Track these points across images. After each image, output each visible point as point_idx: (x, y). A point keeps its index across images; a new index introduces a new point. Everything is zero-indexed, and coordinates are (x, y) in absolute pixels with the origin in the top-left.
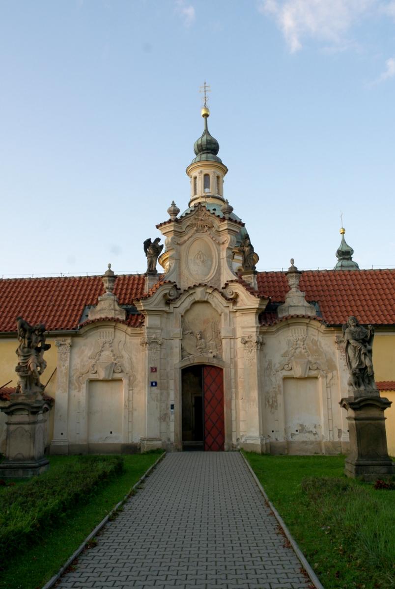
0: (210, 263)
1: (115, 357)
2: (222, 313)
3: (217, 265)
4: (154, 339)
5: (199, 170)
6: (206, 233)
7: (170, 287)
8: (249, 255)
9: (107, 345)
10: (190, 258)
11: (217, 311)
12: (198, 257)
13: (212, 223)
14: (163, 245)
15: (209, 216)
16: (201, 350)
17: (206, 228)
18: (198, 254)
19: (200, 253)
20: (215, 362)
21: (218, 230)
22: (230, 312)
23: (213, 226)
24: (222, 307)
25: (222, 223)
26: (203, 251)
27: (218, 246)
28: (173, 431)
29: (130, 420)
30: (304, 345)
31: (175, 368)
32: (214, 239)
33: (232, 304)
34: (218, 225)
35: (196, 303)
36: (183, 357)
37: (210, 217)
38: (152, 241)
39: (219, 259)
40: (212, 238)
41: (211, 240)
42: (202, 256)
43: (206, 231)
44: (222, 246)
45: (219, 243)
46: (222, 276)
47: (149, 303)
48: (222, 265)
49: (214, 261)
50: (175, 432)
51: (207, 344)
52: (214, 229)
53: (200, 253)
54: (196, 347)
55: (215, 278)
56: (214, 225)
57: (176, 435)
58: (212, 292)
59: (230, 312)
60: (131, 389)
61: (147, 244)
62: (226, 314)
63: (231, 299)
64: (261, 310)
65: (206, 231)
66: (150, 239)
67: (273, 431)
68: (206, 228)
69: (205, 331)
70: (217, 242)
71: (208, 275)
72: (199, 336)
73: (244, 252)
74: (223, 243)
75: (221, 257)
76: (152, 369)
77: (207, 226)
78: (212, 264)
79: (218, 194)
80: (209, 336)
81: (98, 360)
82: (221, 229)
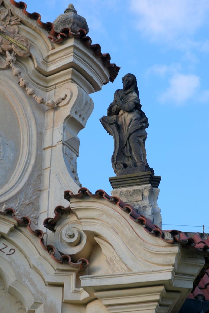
0: (10, 154)
2: (37, 304)
3: (33, 162)
6: (7, 72)
8: (137, 130)
11: (20, 302)
13: (30, 45)
15: (22, 22)
21: (43, 67)
22: (65, 303)
23: (31, 57)
24: (41, 285)
25: (58, 48)
27: (37, 113)
32: (29, 90)
33: (73, 277)
34: (45, 55)
37: (22, 26)
39: (41, 149)
40: (24, 88)
41: (20, 92)
43: (9, 67)
44: (51, 114)
45: (42, 102)
46: (44, 196)
48: (47, 164)
49: (24, 151)
52: (31, 66)
55: (22, 197)
56: (33, 52)
58: (11, 231)
59: (65, 303)
62: (50, 311)
63: (74, 258)
64: (177, 297)
65: (9, 67)
68: (10, 57)
70: (39, 99)
73: (119, 127)
74: (55, 107)
75: (47, 143)
77: (11, 51)
82: (52, 68)
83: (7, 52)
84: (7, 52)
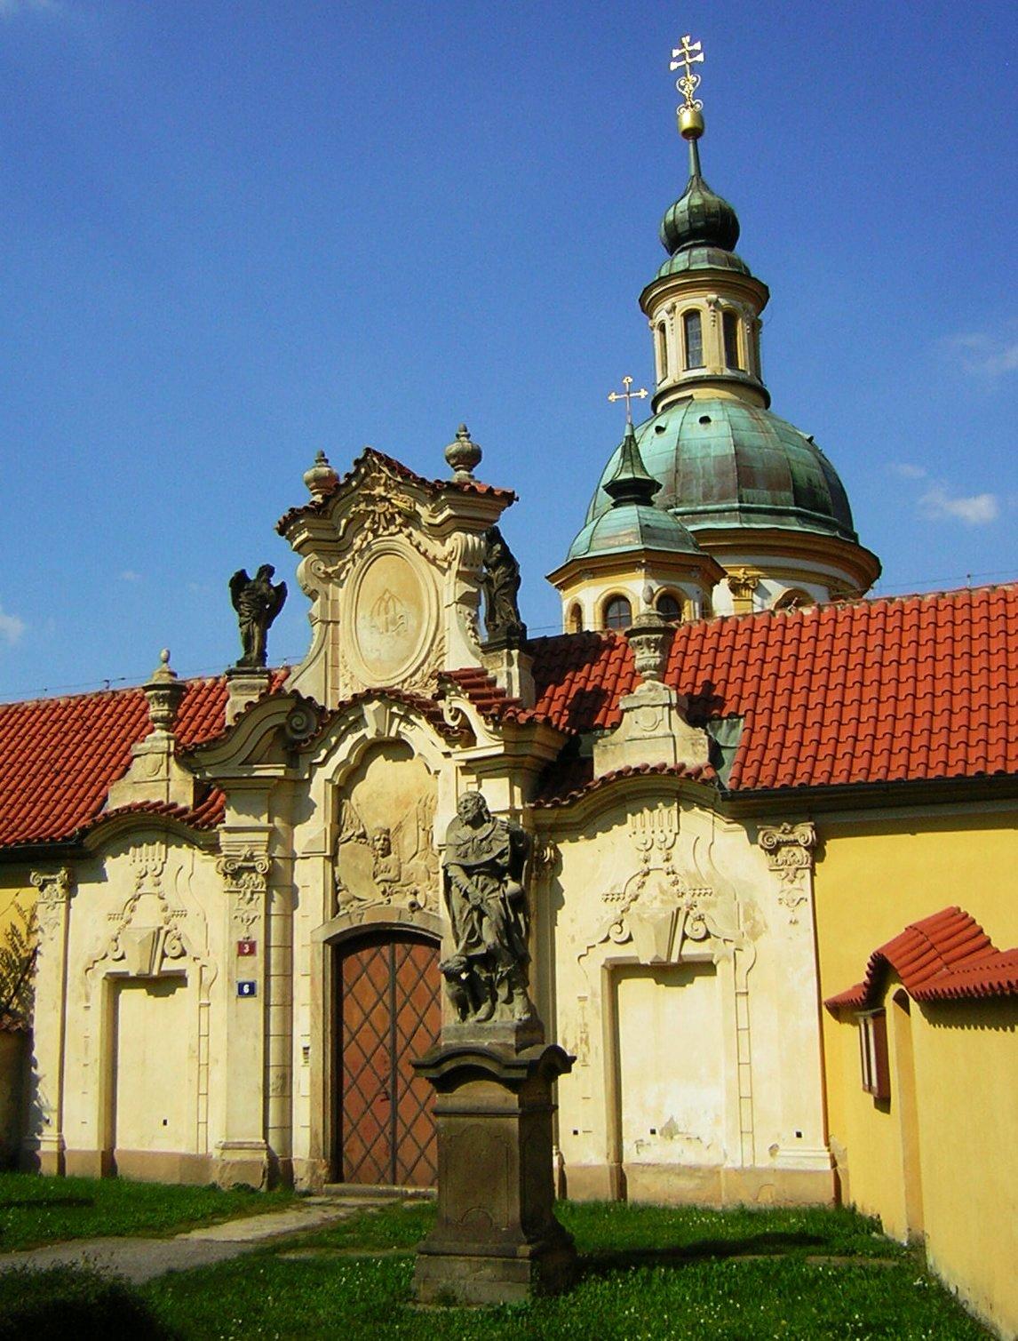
1: (169, 913)
4: (246, 860)
5: (667, 305)
7: (289, 709)
9: (148, 881)
10: (360, 614)
12: (384, 604)
14: (283, 584)
16: (387, 885)
17: (399, 520)
18: (381, 599)
19: (387, 596)
20: (416, 920)
26: (394, 590)
28: (308, 1124)
29: (203, 1091)
30: (667, 860)
31: (313, 942)
32: (422, 550)
35: (371, 750)
36: (336, 909)
38: (252, 575)
42: (391, 603)
47: (220, 760)
50: (311, 1127)
51: (405, 867)
53: (387, 596)
54: (375, 877)
57: (314, 1136)
60: (204, 1001)
61: (239, 582)
65: (401, 531)
66: (243, 572)
67: (576, 1133)
68: (399, 520)
69: (399, 828)
71: (408, 657)
72: (378, 845)
76: (241, 945)
78: (420, 625)
79: (731, 360)
80: (410, 844)
81: (128, 922)
83: (396, 516)
84: (396, 516)
